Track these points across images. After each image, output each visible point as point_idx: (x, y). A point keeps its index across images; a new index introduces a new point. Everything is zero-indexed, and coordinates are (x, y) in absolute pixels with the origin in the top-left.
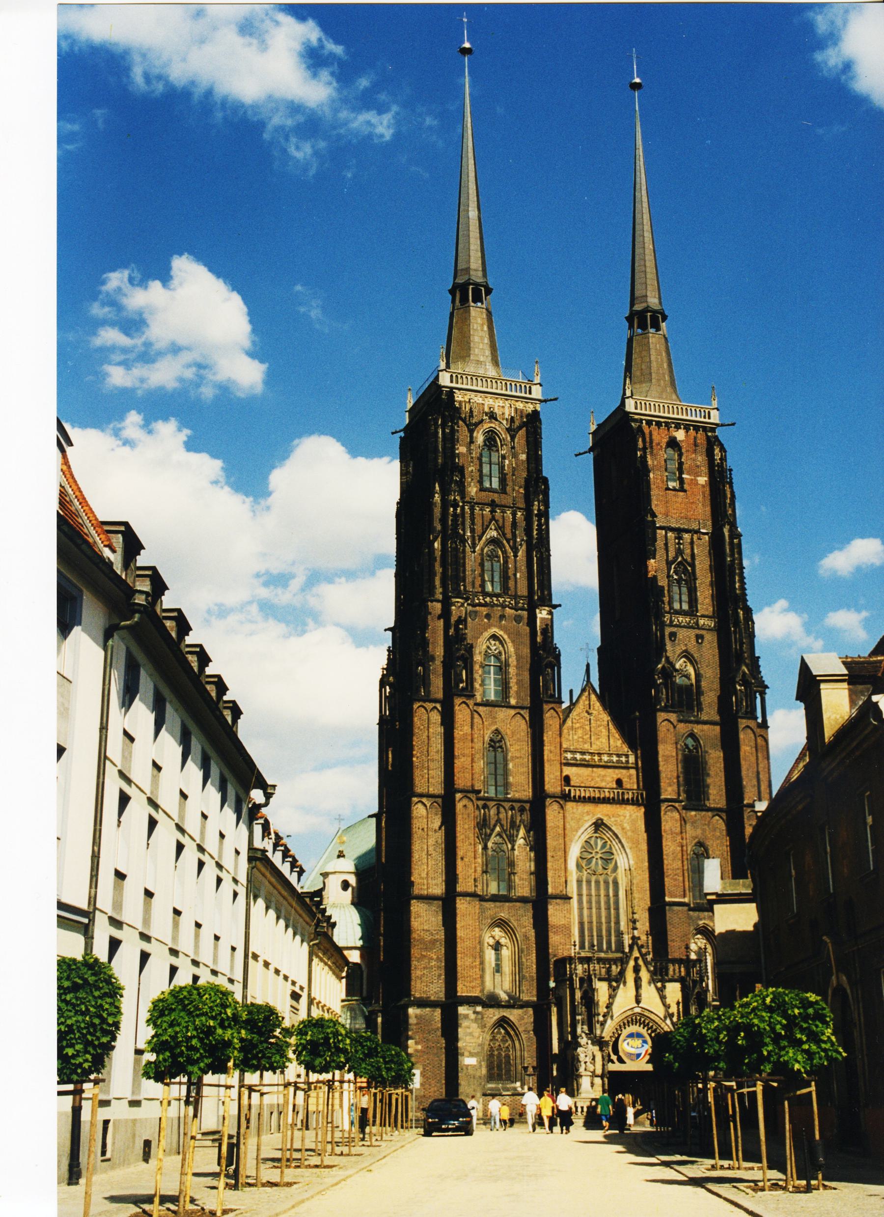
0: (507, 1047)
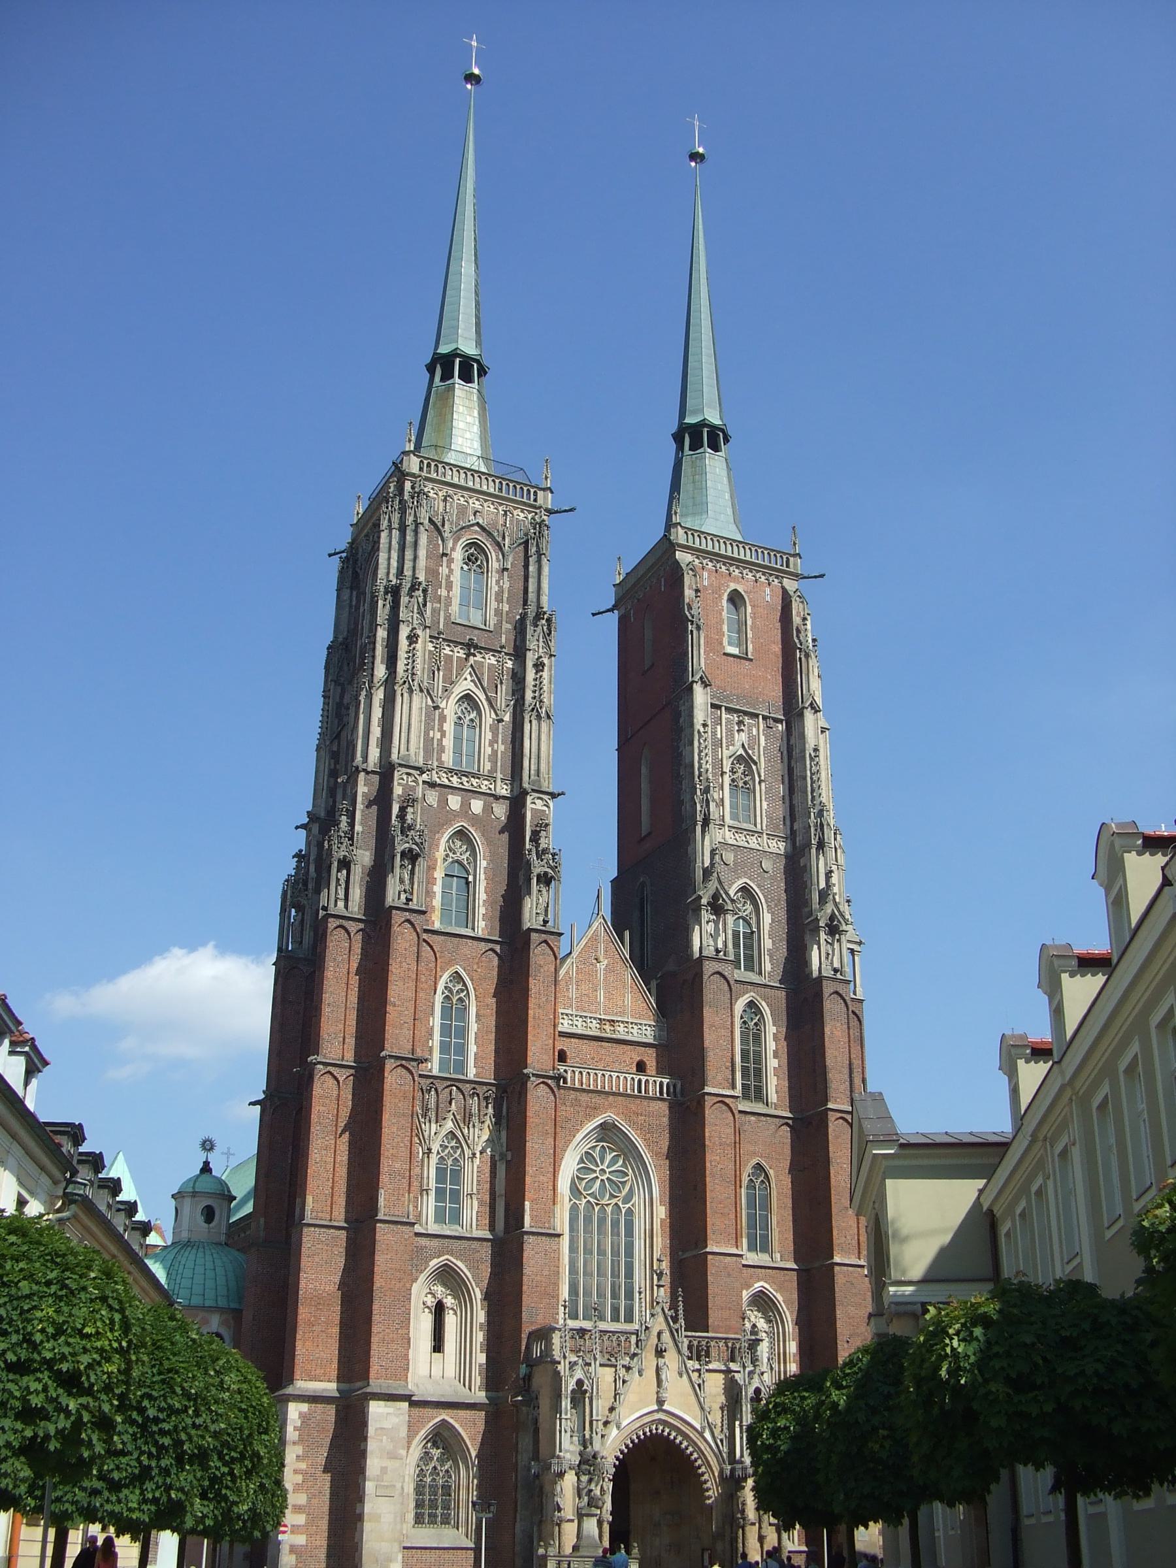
0: (447, 1471)
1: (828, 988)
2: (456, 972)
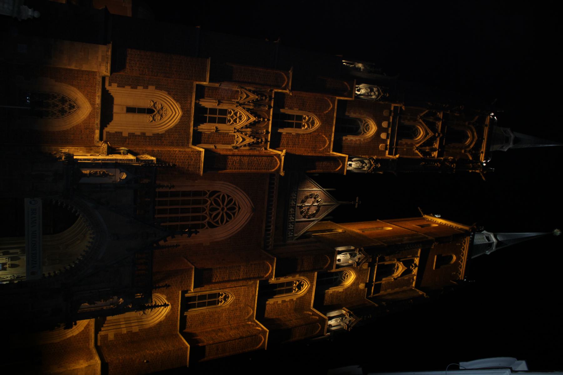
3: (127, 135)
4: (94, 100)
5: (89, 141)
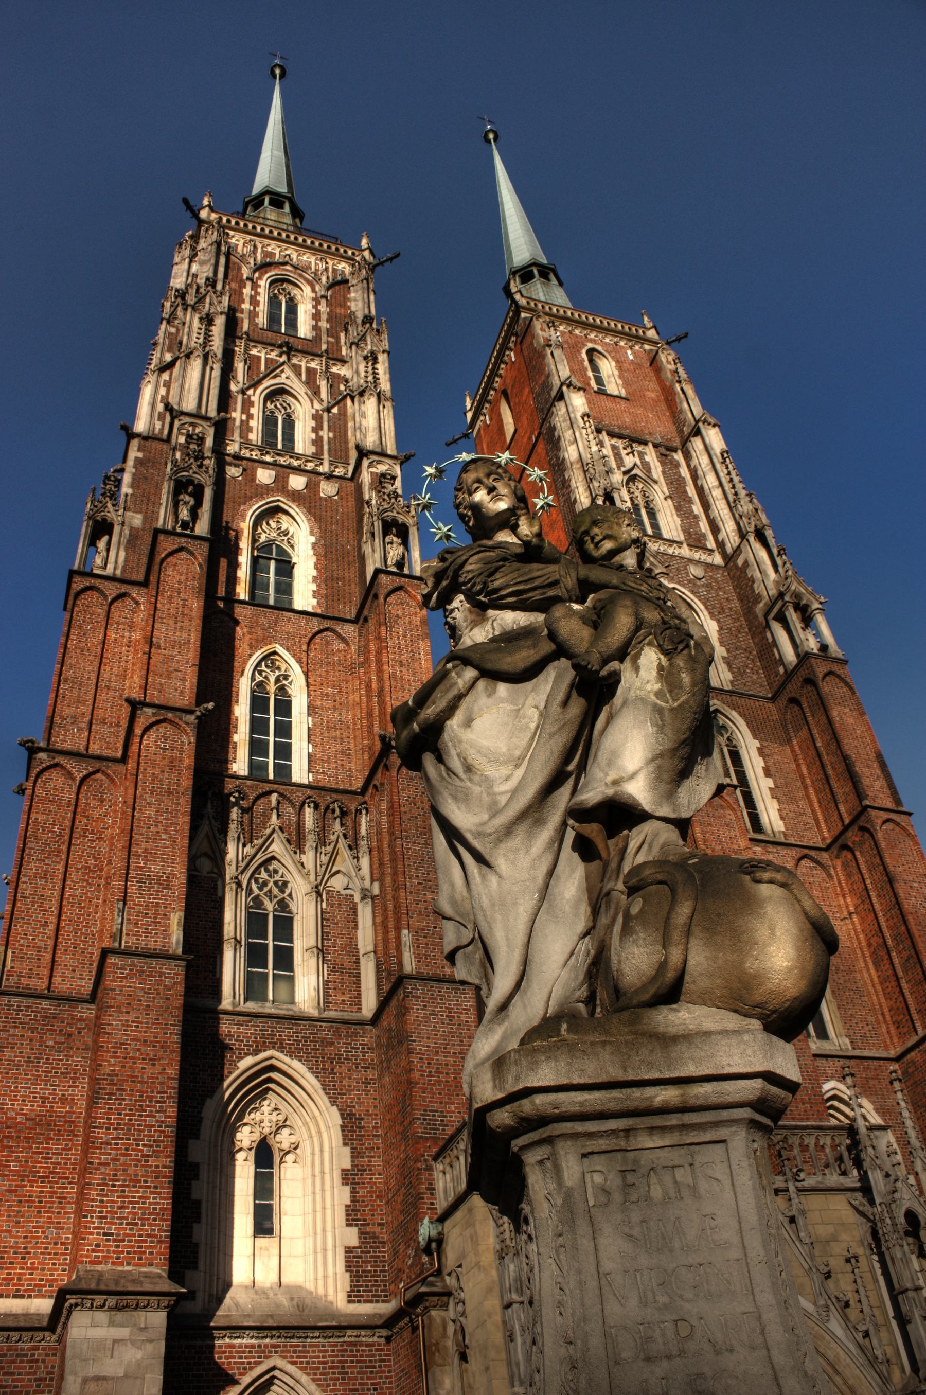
1: (821, 669)
2: (275, 653)
3: (355, 1230)
4: (244, 1352)
5: (384, 1361)
